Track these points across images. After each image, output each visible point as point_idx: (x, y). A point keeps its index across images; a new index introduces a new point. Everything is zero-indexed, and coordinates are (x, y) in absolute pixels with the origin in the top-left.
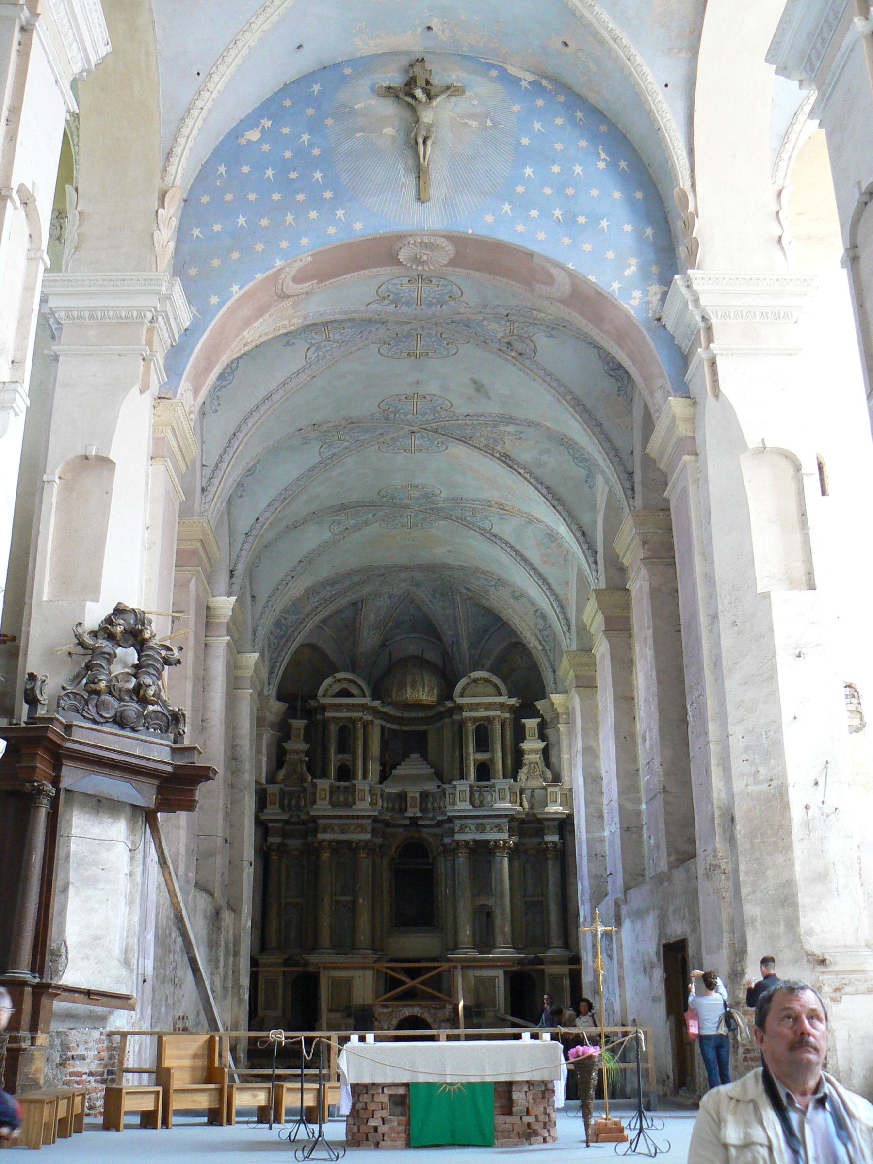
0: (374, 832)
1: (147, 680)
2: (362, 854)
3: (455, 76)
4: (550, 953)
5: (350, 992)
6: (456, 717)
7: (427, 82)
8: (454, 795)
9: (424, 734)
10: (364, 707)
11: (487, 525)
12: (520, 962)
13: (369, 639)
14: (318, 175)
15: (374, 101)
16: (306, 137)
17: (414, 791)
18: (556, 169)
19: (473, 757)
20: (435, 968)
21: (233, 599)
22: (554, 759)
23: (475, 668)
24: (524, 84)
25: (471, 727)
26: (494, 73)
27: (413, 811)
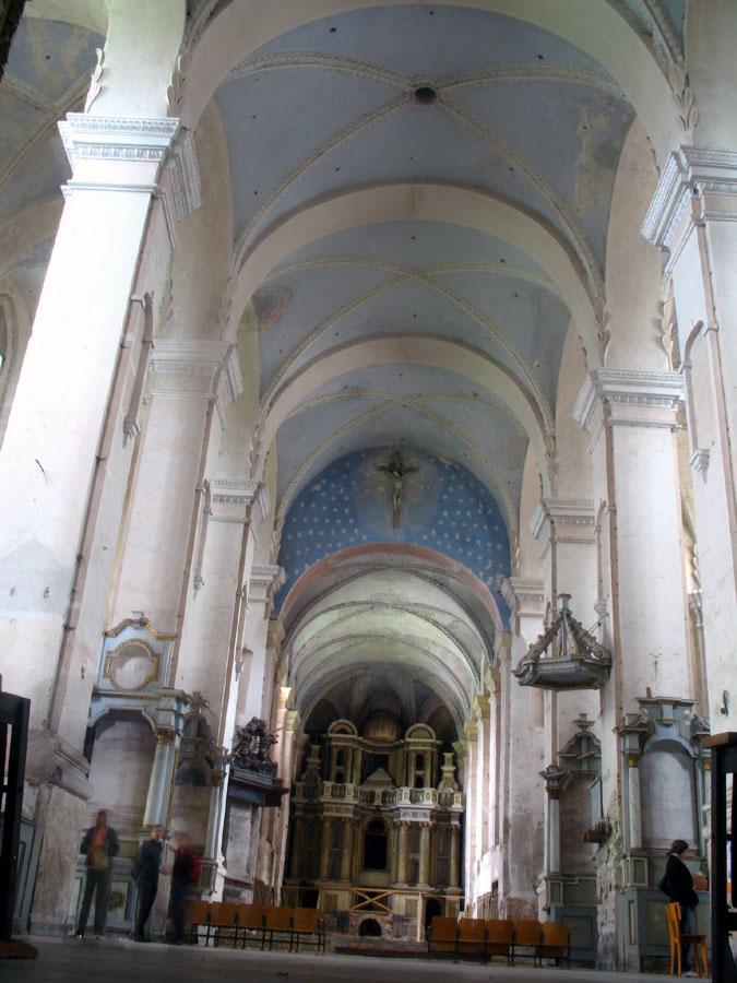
0: (355, 813)
1: (264, 750)
2: (348, 825)
3: (413, 461)
4: (449, 889)
5: (336, 904)
6: (406, 749)
7: (401, 465)
8: (401, 794)
9: (388, 756)
10: (354, 740)
11: (426, 648)
12: (432, 892)
13: (358, 698)
14: (347, 510)
15: (375, 473)
16: (342, 490)
17: (379, 791)
18: (458, 513)
19: (413, 773)
20: (380, 893)
21: (290, 689)
22: (461, 778)
23: (418, 722)
24: (446, 467)
25: (413, 755)
26: (433, 460)
27: (378, 802)
